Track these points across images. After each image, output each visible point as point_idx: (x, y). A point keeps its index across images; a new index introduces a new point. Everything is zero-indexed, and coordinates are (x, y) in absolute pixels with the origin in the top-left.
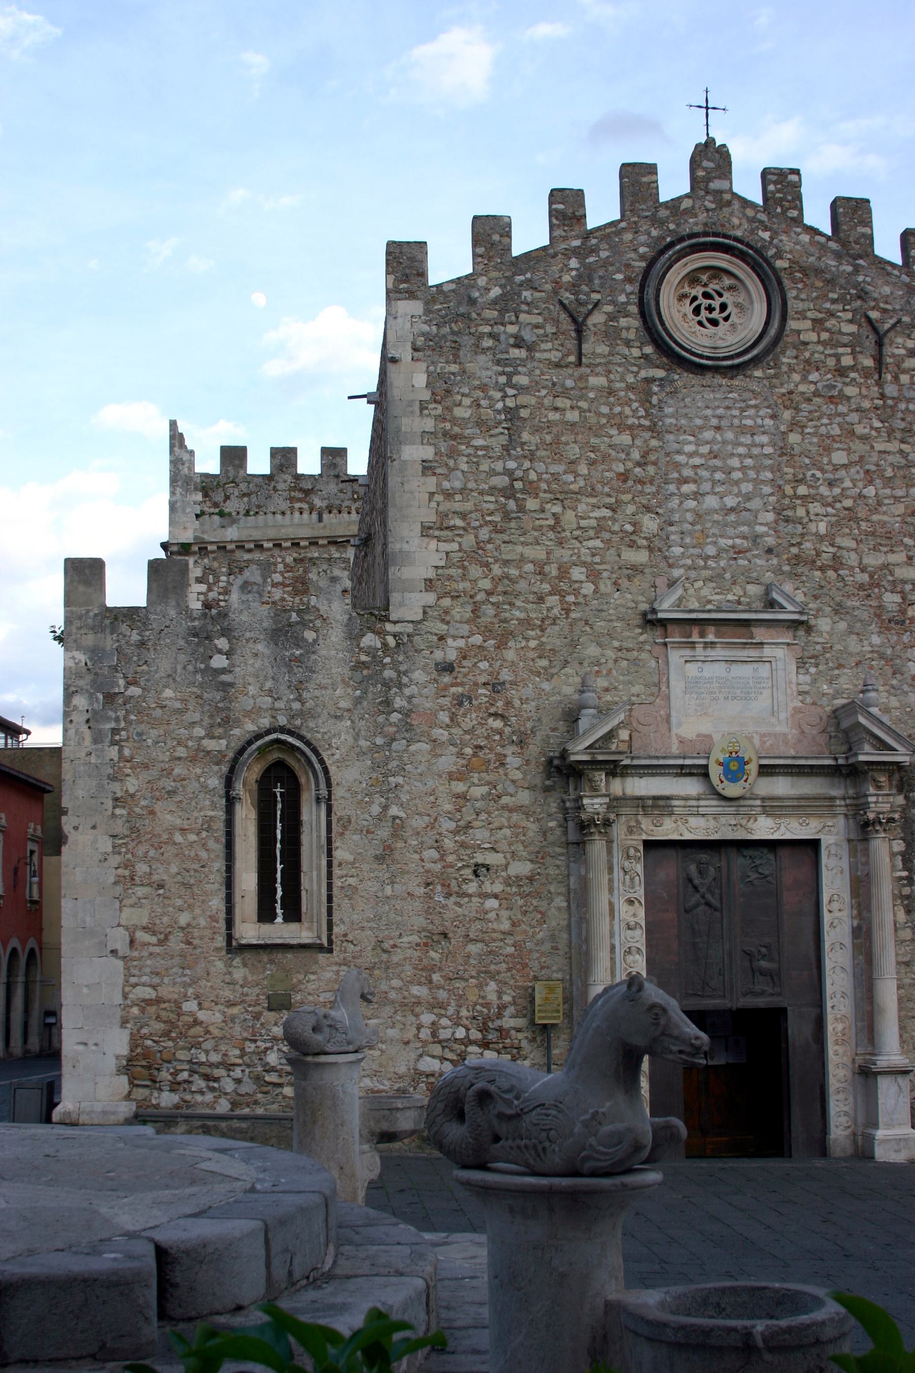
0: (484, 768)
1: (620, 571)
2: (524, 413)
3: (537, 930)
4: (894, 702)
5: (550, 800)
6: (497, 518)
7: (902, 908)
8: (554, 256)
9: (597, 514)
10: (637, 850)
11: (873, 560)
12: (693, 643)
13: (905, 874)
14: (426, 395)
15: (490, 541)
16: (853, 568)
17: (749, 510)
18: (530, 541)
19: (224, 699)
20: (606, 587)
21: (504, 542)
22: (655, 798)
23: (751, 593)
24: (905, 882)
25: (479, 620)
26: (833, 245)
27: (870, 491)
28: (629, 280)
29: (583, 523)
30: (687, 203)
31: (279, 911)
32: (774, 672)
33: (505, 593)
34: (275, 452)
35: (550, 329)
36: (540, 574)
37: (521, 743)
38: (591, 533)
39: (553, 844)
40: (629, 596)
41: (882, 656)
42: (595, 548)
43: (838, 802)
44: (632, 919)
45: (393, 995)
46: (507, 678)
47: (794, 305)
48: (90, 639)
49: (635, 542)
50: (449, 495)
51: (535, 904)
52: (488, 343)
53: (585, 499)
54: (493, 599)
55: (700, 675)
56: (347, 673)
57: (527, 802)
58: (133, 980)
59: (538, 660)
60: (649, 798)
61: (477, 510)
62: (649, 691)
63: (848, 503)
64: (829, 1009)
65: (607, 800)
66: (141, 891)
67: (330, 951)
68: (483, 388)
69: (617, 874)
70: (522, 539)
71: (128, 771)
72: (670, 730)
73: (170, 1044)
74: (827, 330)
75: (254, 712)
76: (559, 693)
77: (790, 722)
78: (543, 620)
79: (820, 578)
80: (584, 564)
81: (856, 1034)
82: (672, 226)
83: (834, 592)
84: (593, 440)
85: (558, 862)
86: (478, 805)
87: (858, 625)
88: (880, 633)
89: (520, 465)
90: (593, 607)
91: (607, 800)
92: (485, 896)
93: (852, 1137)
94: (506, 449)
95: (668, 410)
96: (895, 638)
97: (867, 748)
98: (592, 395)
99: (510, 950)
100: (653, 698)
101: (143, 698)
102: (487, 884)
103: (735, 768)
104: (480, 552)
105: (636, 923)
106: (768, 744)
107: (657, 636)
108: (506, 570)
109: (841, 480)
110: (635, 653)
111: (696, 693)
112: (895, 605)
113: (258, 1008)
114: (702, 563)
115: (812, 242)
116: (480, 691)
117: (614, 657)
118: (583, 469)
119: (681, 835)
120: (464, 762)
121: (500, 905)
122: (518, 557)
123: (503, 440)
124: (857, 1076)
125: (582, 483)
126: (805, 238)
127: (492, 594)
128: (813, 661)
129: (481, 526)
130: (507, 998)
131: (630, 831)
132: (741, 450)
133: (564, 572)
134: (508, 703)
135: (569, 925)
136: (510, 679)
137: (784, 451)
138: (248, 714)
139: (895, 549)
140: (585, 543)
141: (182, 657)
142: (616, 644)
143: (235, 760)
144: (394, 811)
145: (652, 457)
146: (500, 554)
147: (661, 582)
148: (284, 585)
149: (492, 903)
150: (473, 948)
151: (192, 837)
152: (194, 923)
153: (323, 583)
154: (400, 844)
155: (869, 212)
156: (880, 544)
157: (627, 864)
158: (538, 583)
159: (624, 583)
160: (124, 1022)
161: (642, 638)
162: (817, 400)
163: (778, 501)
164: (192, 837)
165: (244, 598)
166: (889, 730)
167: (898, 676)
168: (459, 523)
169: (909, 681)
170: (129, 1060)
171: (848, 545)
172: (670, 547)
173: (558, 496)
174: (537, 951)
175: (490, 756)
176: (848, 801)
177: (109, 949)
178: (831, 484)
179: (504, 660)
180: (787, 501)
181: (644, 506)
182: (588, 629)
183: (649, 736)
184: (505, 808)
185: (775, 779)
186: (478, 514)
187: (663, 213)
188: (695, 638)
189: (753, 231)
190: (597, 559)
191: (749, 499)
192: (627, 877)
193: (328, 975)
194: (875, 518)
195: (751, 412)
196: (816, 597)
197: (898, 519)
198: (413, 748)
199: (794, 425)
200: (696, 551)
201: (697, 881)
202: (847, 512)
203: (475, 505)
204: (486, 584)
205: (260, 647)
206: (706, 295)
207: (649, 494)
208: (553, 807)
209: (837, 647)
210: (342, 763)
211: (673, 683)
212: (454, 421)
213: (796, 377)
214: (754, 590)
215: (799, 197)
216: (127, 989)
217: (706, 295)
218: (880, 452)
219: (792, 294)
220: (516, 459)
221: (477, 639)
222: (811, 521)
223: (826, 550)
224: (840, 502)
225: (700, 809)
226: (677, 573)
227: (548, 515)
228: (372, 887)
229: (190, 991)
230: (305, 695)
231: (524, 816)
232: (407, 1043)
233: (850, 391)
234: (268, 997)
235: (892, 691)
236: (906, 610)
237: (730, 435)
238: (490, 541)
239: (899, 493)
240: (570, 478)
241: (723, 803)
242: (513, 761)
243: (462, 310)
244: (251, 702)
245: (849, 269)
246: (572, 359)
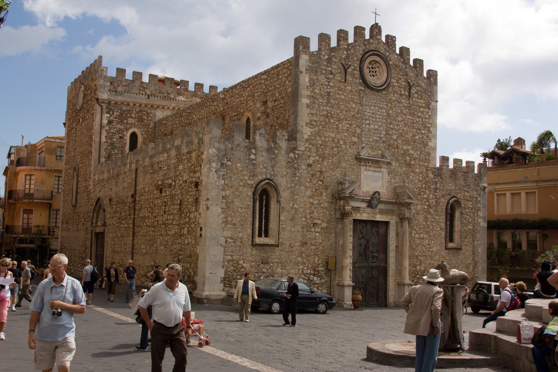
2: (332, 94)
8: (341, 49)
11: (405, 147)
14: (308, 84)
15: (321, 130)
18: (331, 131)
19: (254, 168)
22: (357, 207)
26: (402, 60)
27: (405, 129)
28: (357, 60)
29: (344, 128)
30: (371, 41)
31: (263, 234)
33: (324, 145)
34: (134, 73)
35: (339, 71)
37: (326, 189)
38: (345, 131)
41: (405, 174)
45: (293, 260)
47: (393, 75)
48: (217, 145)
50: (312, 115)
52: (324, 72)
53: (344, 121)
54: (322, 147)
56: (286, 164)
58: (226, 254)
63: (401, 131)
65: (351, 207)
66: (229, 226)
67: (278, 246)
68: (322, 85)
71: (227, 188)
72: (360, 189)
73: (236, 274)
74: (399, 83)
75: (262, 173)
80: (343, 140)
82: (368, 47)
83: (396, 155)
84: (347, 105)
86: (316, 206)
88: (405, 167)
89: (330, 109)
91: (351, 207)
92: (316, 232)
94: (327, 104)
95: (364, 99)
97: (406, 198)
98: (347, 92)
99: (321, 248)
101: (232, 165)
102: (317, 228)
109: (399, 125)
113: (259, 263)
115: (397, 58)
118: (344, 113)
120: (312, 193)
123: (326, 101)
125: (343, 116)
126: (396, 56)
130: (320, 262)
132: (379, 113)
133: (338, 142)
134: (324, 177)
135: (336, 243)
137: (388, 115)
138: (260, 174)
141: (243, 154)
142: (349, 163)
143: (256, 187)
144: (296, 206)
145: (360, 112)
147: (360, 147)
148: (135, 118)
149: (318, 234)
150: (313, 247)
151: (244, 210)
152: (243, 237)
153: (281, 136)
154: (296, 216)
155: (409, 52)
159: (351, 146)
160: (223, 267)
161: (355, 162)
162: (396, 102)
164: (244, 210)
165: (260, 138)
166: (413, 195)
168: (315, 123)
170: (224, 279)
177: (220, 243)
178: (397, 125)
180: (388, 129)
184: (322, 207)
187: (366, 42)
189: (385, 52)
190: (346, 139)
193: (277, 254)
194: (406, 136)
195: (382, 103)
198: (301, 188)
199: (391, 108)
200: (368, 140)
201: (362, 231)
204: (320, 142)
205: (264, 154)
206: (372, 68)
209: (396, 170)
210: (283, 191)
212: (315, 93)
213: (392, 95)
214: (380, 152)
215: (395, 45)
216: (224, 256)
217: (372, 68)
218: (408, 119)
219: (392, 71)
220: (329, 107)
221: (317, 158)
228: (289, 228)
229: (241, 257)
230: (275, 169)
232: (296, 274)
233: (403, 101)
234: (262, 260)
237: (377, 109)
238: (321, 130)
239: (411, 130)
240: (341, 114)
242: (324, 194)
243: (318, 60)
244: (260, 170)
245: (405, 67)
246: (343, 80)
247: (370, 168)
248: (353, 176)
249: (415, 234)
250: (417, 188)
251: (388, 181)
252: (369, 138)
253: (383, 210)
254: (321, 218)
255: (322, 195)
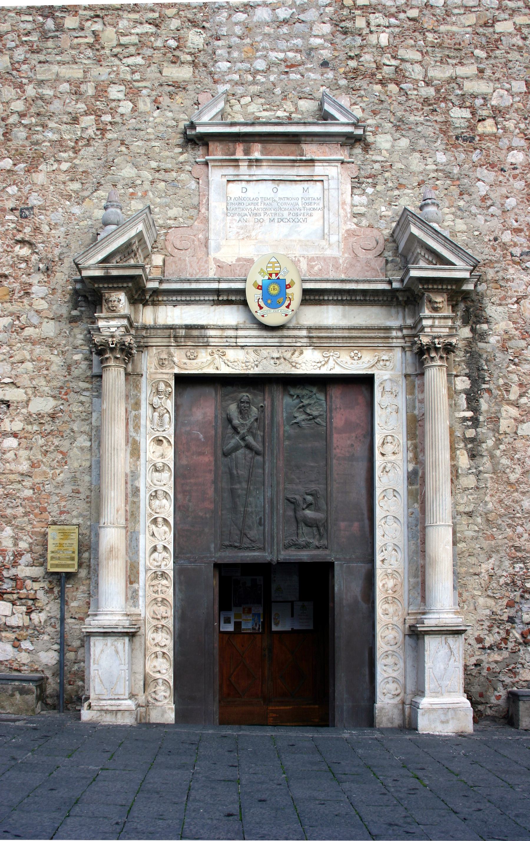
0: (8, 297)
1: (161, 89)
3: (58, 471)
4: (460, 225)
5: (76, 331)
6: (34, 38)
7: (465, 452)
9: (139, 30)
10: (168, 385)
12: (237, 160)
13: (469, 414)
16: (417, 81)
17: (303, 21)
18: (65, 57)
20: (145, 105)
21: (40, 62)
23: (304, 109)
24: (470, 423)
25: (9, 143)
29: (124, 40)
32: (326, 192)
33: (38, 115)
36: (76, 93)
39: (78, 378)
40: (170, 114)
41: (448, 175)
42: (135, 66)
43: (394, 333)
44: (160, 460)
46: (36, 202)
49: (178, 57)
51: (56, 443)
53: (125, 15)
55: (243, 195)
57: (52, 334)
59: (69, 183)
60: (181, 327)
61: (13, 31)
62: (187, 214)
63: (413, 13)
64: (378, 563)
69: (145, 410)
70: (58, 58)
72: (208, 254)
76: (90, 218)
77: (342, 245)
78: (76, 143)
79: (380, 92)
80: (123, 82)
81: (409, 590)
85: (82, 398)
87: (422, 142)
90: (130, 127)
93: (400, 707)
96: (463, 156)
100: (192, 221)
103: (274, 292)
104: (14, 73)
105: (164, 465)
106: (316, 268)
107: (199, 155)
108: (40, 91)
110: (174, 174)
111: (239, 215)
112: (463, 120)
114: (250, 78)
116: (7, 217)
117: (151, 178)
119: (217, 368)
121: (19, 444)
122: (54, 77)
124: (407, 637)
127: (25, 115)
128: (370, 180)
129: (17, 46)
131: (161, 364)
134: (37, 229)
135: (90, 467)
136: (40, 203)
139: (464, 61)
140: (125, 60)
142: (154, 164)
146: (35, 75)
156: (448, 56)
157: (156, 400)
158: (74, 103)
159: (165, 101)
161: (182, 158)
163: (336, 11)
167: (465, 197)
169: (479, 203)
171: (412, 57)
172: (216, 62)
173: (99, 13)
174: (57, 494)
175: (15, 285)
176: (405, 332)
179: (34, 184)
181: (189, 20)
182: (123, 148)
183: (185, 260)
185: (324, 308)
186: (14, 35)
188: (239, 155)
190: (137, 76)
191: (304, 11)
192: (156, 414)
194: (443, 28)
196: (375, 113)
197: (469, 30)
200: (245, 66)
202: (412, 23)
203: (12, 25)
204: (19, 106)
207: (195, 8)
208: (79, 338)
211: (212, 204)
214: (306, 105)
222: (371, 32)
223: (388, 63)
224: (405, 12)
225: (238, 340)
226: (222, 88)
227: (88, 33)
231: (47, 349)
235: (459, 213)
236: (475, 126)
238: (25, 61)
241: (264, 333)
247: (255, 171)
248: (172, 213)
249: (519, 421)
250: (517, 231)
251: (355, 215)
252: (249, 60)
253: (327, 328)
254: (24, 380)
255: (27, 294)
